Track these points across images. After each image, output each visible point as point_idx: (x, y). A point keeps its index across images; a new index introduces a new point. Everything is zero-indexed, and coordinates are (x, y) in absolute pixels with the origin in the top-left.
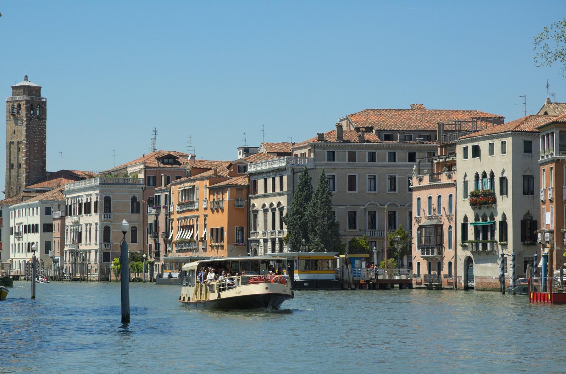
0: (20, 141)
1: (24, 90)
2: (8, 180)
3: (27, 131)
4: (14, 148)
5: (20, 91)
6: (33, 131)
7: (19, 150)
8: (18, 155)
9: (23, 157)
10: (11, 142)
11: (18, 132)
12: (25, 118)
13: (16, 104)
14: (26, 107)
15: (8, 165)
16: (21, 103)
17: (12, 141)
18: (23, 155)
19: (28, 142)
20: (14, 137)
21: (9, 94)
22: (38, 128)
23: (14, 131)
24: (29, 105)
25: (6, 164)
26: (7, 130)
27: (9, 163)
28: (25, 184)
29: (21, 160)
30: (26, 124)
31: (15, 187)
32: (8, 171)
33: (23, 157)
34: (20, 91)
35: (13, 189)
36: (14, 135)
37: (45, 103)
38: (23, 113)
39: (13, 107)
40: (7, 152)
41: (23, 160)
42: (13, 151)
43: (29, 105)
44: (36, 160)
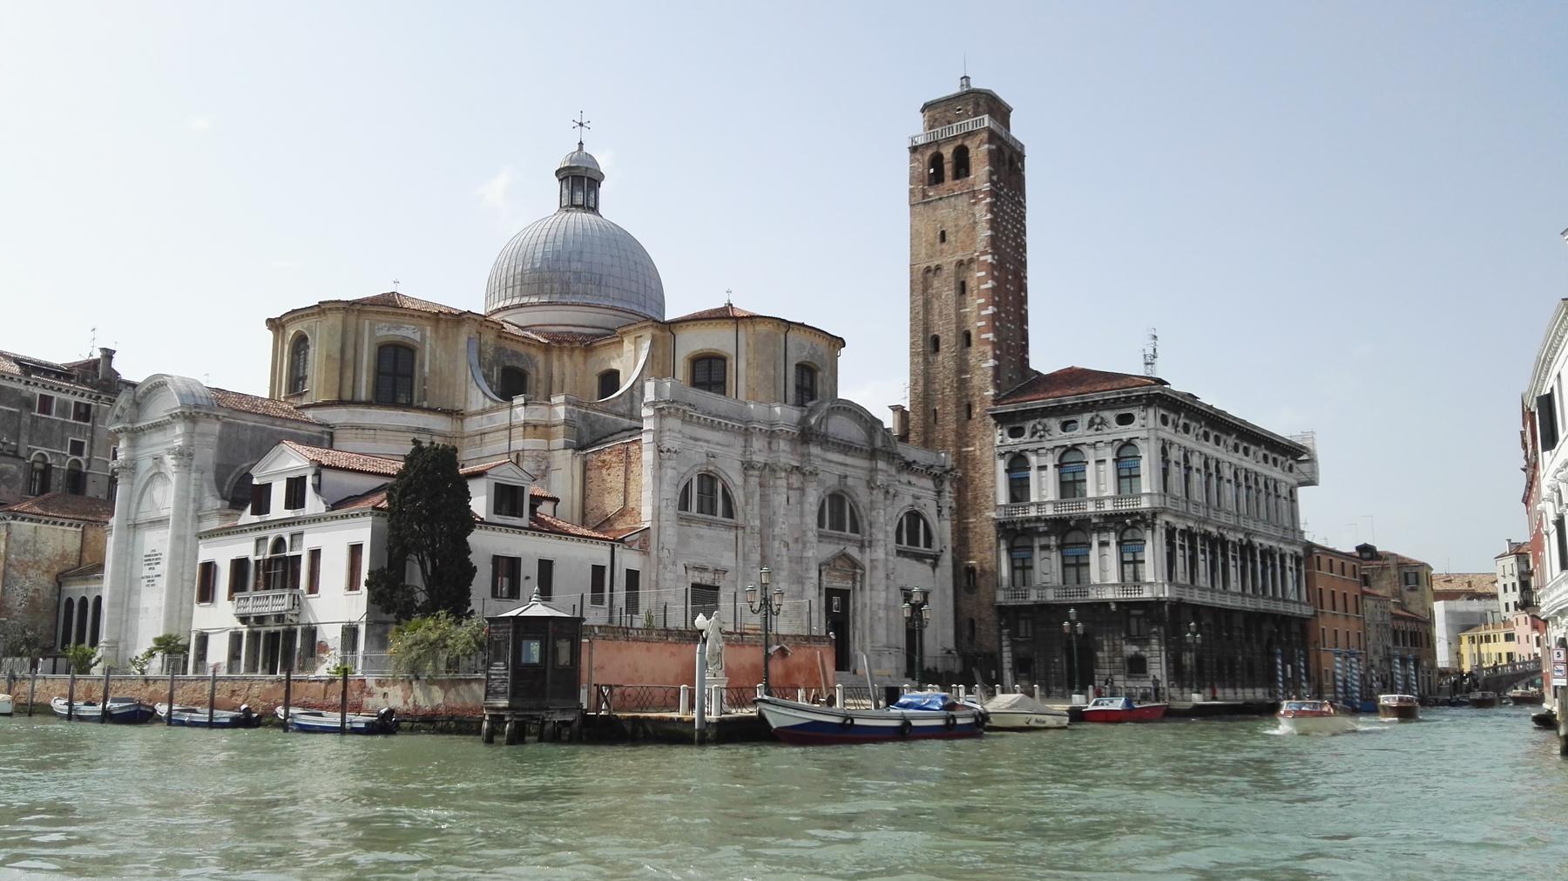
0: (966, 259)
1: (977, 105)
2: (920, 388)
3: (993, 224)
4: (945, 290)
5: (959, 110)
6: (1003, 233)
7: (962, 288)
8: (960, 304)
9: (982, 307)
10: (928, 270)
11: (957, 232)
12: (986, 186)
13: (948, 152)
14: (990, 152)
15: (920, 342)
16: (967, 143)
17: (933, 267)
18: (982, 301)
19: (994, 262)
20: (942, 251)
21: (917, 128)
22: (1014, 227)
23: (943, 233)
24: (994, 147)
25: (911, 338)
26: (915, 235)
27: (921, 335)
28: (991, 392)
29: (972, 320)
30: (992, 205)
31: (951, 408)
32: (921, 360)
33: (982, 307)
34: (959, 110)
35: (939, 416)
36: (944, 246)
37: (1021, 157)
38: (980, 171)
39: (937, 161)
40: (912, 303)
41: (980, 318)
42: (939, 296)
43: (994, 147)
44: (1009, 321)
